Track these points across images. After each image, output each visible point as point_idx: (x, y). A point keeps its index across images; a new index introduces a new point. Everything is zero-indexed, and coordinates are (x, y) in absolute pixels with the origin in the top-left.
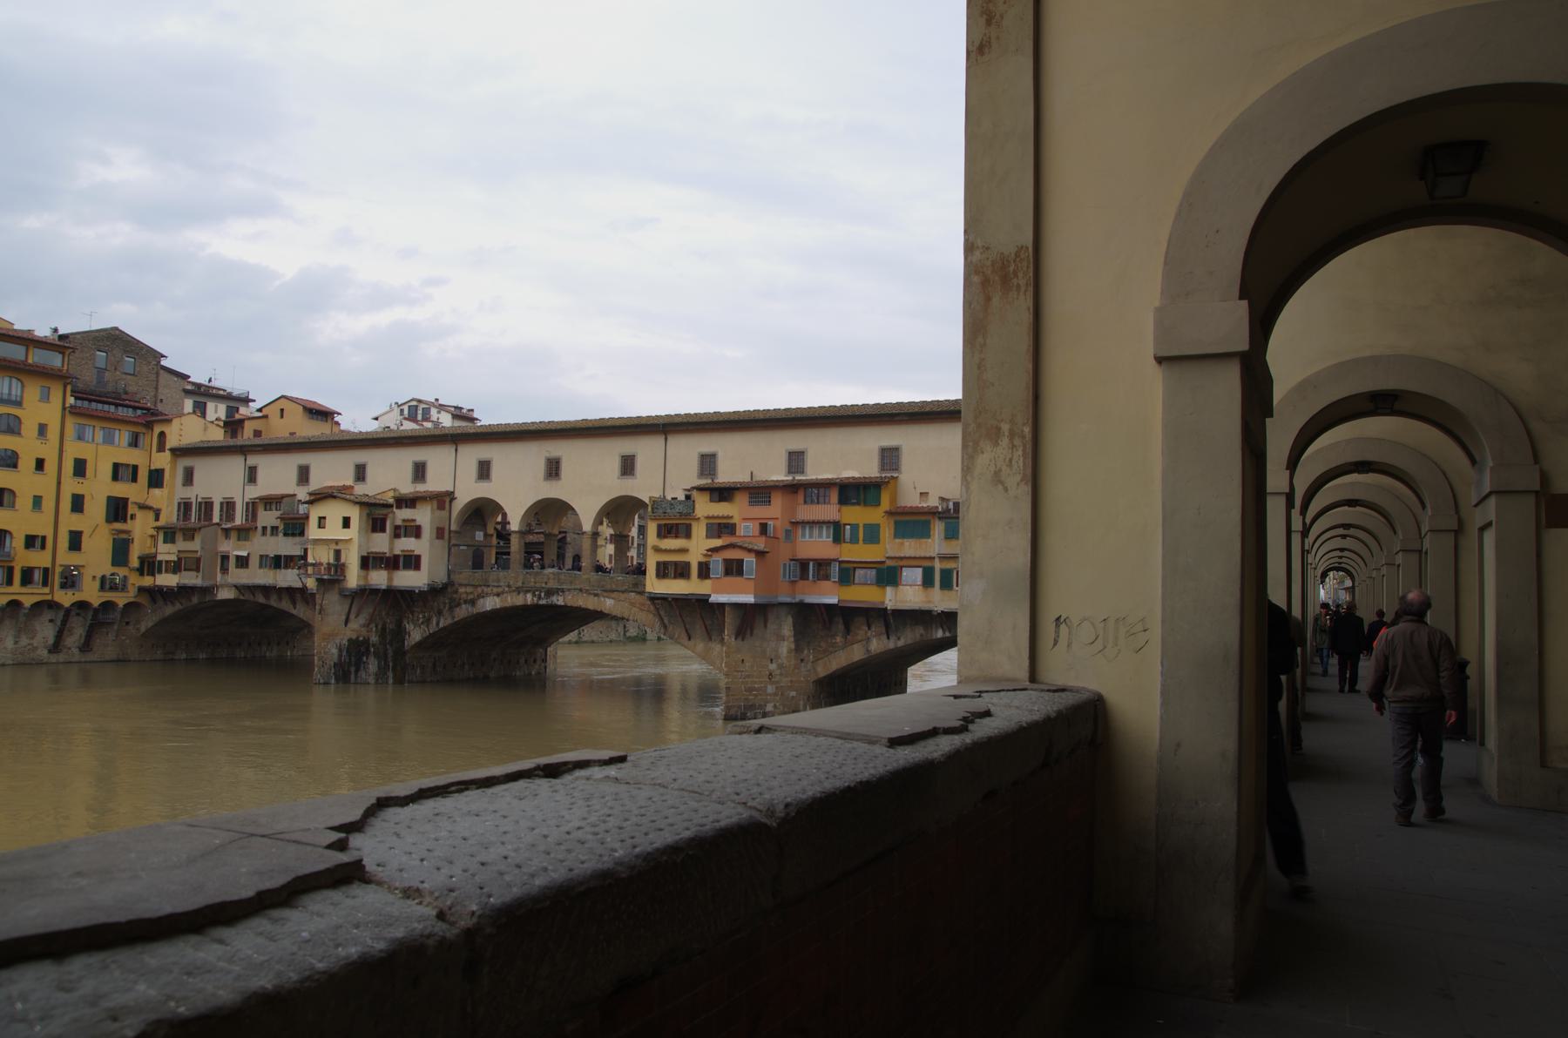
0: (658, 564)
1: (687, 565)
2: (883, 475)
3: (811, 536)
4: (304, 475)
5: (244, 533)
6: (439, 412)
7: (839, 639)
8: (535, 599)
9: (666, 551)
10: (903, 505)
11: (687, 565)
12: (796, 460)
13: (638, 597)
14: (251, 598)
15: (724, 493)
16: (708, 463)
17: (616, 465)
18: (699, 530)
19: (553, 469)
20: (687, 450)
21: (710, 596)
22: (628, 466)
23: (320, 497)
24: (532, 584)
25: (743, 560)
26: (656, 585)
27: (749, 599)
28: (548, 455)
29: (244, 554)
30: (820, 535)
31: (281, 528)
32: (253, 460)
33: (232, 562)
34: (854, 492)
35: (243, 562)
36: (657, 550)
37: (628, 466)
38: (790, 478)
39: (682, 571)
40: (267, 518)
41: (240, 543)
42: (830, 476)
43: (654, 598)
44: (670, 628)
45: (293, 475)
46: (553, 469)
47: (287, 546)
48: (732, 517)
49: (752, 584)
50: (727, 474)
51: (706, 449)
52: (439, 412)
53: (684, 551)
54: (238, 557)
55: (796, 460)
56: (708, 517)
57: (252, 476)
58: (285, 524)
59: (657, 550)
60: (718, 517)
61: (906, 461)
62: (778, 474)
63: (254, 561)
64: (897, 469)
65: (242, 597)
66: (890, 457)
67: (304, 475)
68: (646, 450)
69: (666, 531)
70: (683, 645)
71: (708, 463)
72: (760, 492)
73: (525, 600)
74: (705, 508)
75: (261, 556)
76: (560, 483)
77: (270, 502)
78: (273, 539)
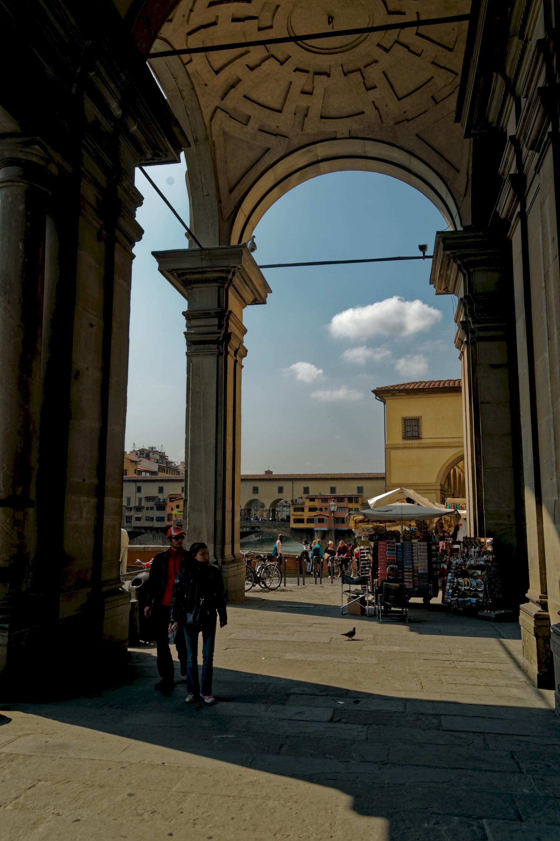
0: (294, 519)
1: (303, 519)
2: (359, 494)
3: (339, 511)
4: (161, 490)
5: (139, 509)
6: (153, 454)
7: (347, 539)
8: (250, 530)
9: (295, 515)
10: (364, 502)
11: (303, 519)
12: (333, 490)
13: (285, 529)
14: (139, 531)
15: (312, 500)
16: (306, 490)
17: (276, 490)
18: (306, 510)
19: (256, 490)
20: (299, 486)
21: (314, 528)
22: (281, 490)
23: (172, 499)
24: (249, 525)
25: (324, 519)
26: (293, 525)
27: (326, 529)
28: (254, 486)
29: (140, 516)
30: (342, 511)
31: (155, 508)
32: (139, 484)
33: (133, 519)
34: (350, 499)
35: (138, 519)
36: (293, 515)
37: (281, 490)
38: (332, 495)
39: (301, 521)
40: (151, 504)
41: (137, 512)
42: (342, 494)
43: (293, 529)
44: (296, 537)
45: (157, 490)
46: (256, 490)
47: (156, 514)
48: (316, 506)
49: (326, 525)
50: (312, 493)
51: (306, 486)
52: (153, 454)
53: (302, 515)
54: (136, 517)
55: (333, 490)
56: (309, 506)
57: (139, 490)
58: (157, 507)
59: (293, 515)
60: (312, 506)
61: (365, 490)
62: (328, 493)
63: (144, 519)
64: (362, 493)
65: (135, 531)
66: (360, 490)
67: (161, 490)
68: (287, 486)
69: (295, 510)
70: (299, 542)
71: (306, 490)
72: (325, 500)
73: (247, 530)
74: (308, 504)
75: (146, 517)
76: (258, 494)
77: (148, 499)
78: (151, 511)
